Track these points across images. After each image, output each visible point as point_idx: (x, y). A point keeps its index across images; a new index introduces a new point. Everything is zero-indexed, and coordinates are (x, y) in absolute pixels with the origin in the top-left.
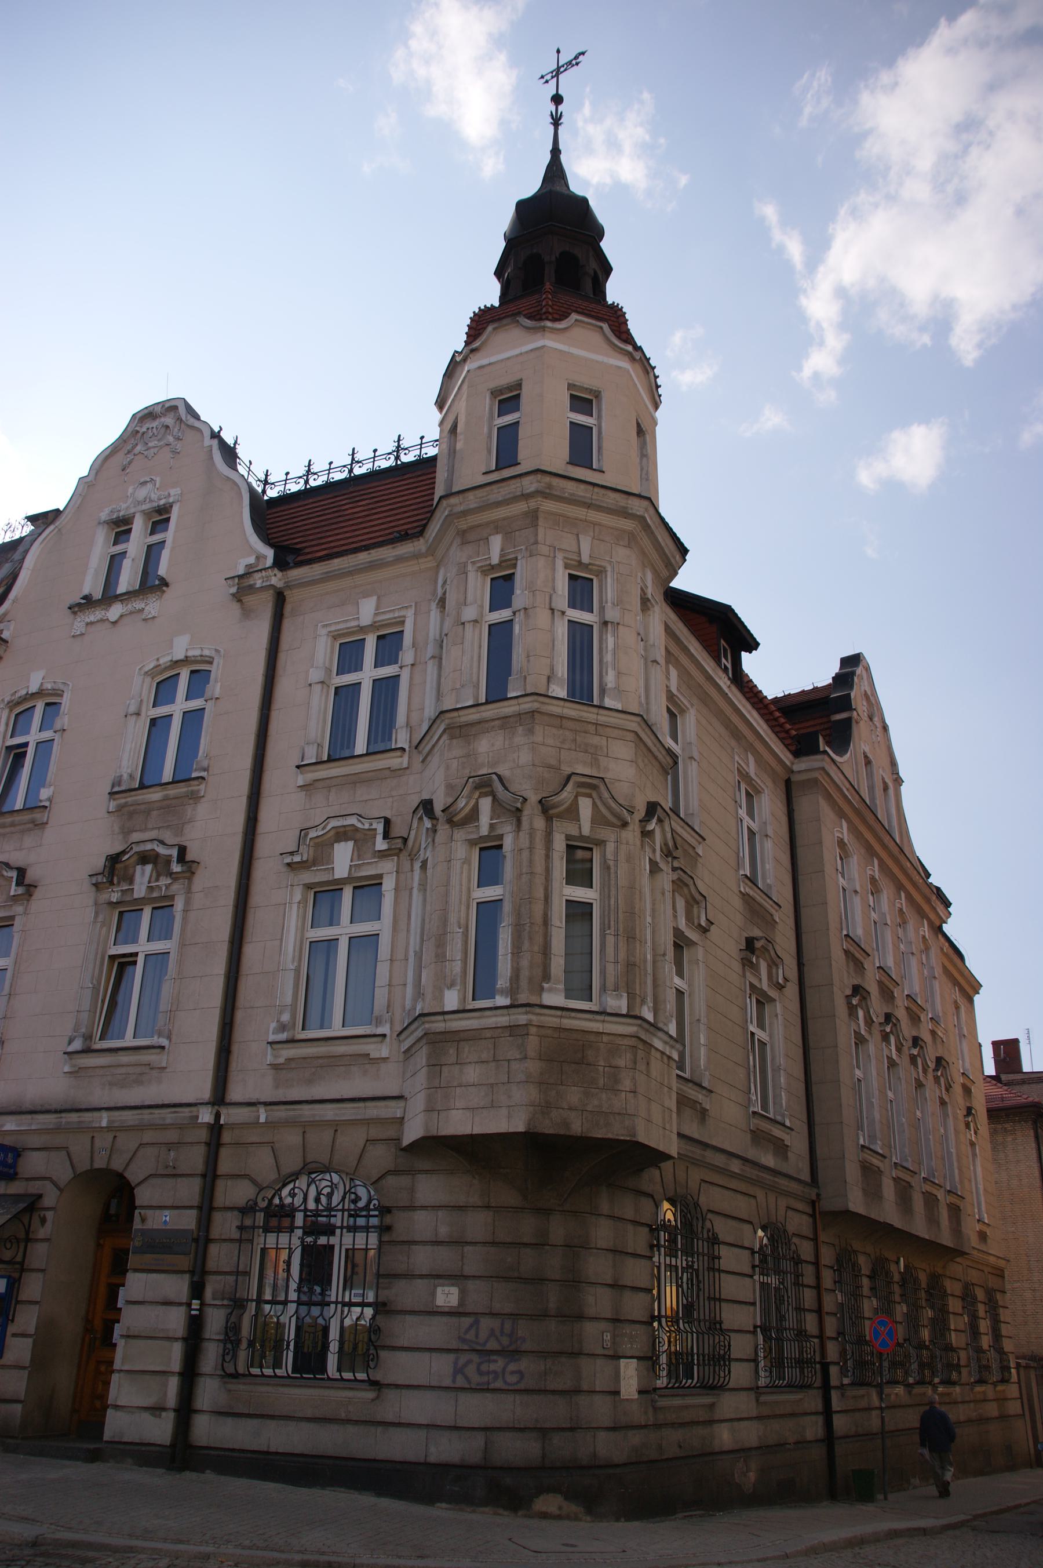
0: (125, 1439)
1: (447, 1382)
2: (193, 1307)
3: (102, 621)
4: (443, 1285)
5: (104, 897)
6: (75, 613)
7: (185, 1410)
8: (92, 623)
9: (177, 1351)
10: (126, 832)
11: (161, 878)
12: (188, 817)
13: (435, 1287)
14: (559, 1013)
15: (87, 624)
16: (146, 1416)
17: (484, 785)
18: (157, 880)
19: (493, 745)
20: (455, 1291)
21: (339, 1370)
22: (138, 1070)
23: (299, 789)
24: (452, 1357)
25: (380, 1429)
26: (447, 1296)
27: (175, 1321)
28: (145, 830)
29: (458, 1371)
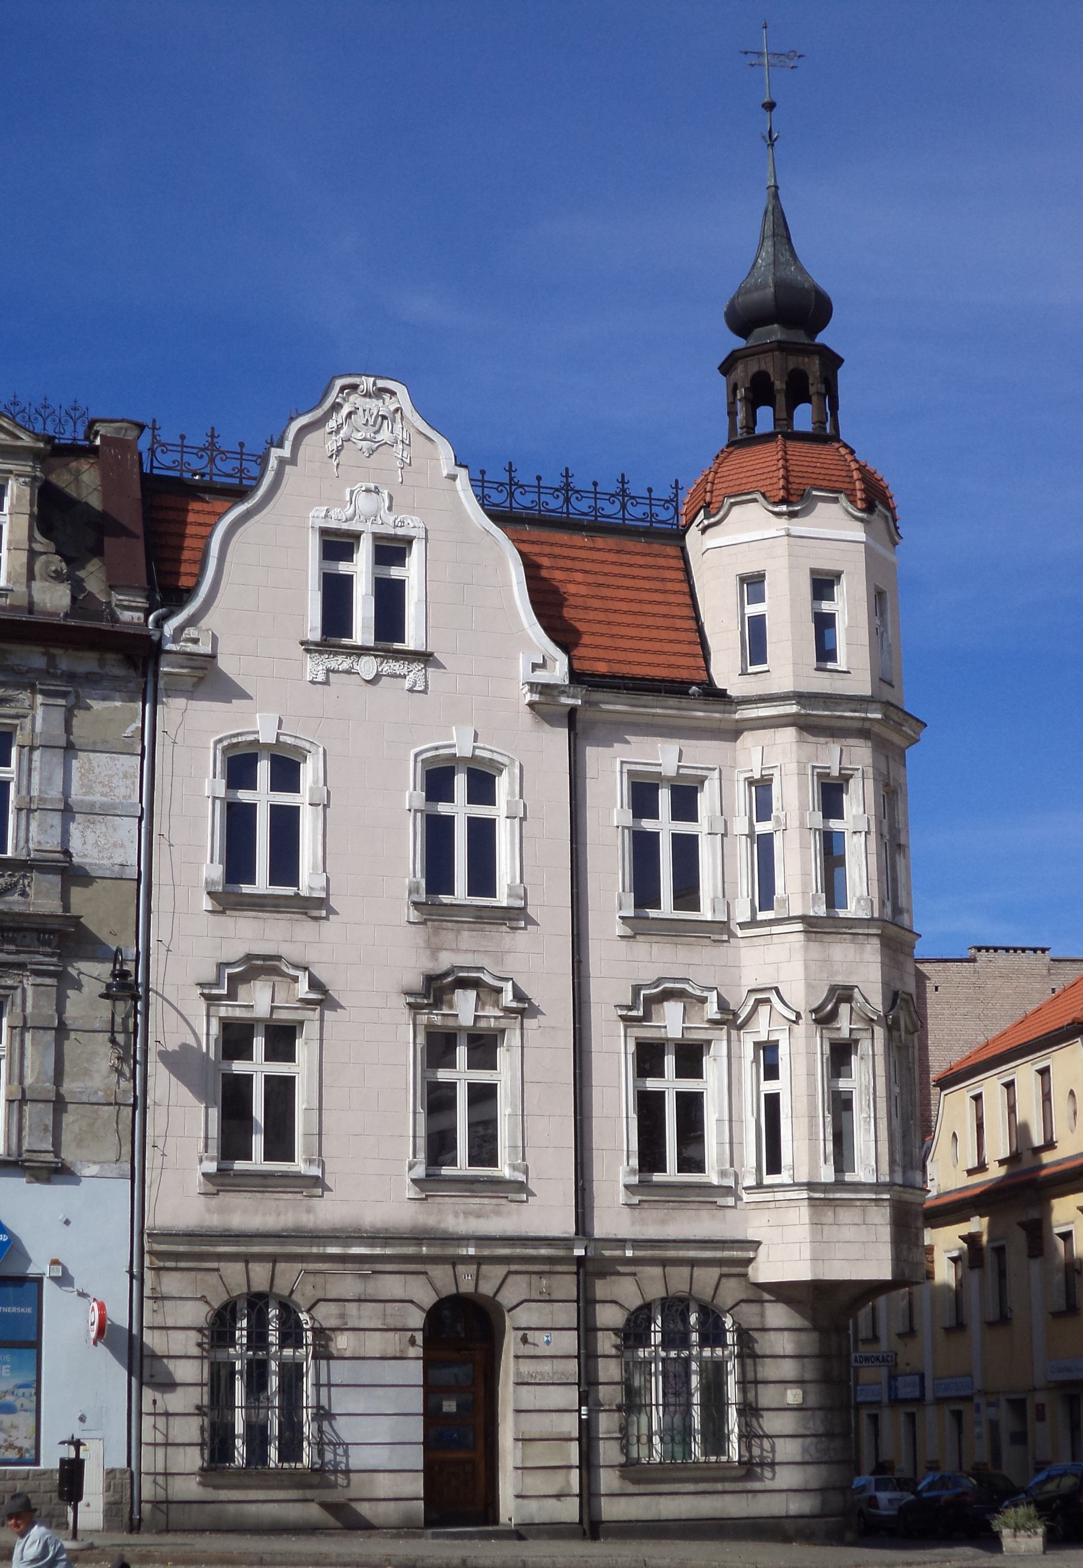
0: (537, 1521)
1: (798, 1459)
2: (583, 1412)
3: (348, 672)
4: (791, 1389)
5: (423, 1019)
7: (588, 1494)
8: (333, 671)
9: (574, 1447)
10: (434, 951)
11: (487, 1008)
12: (507, 947)
13: (786, 1390)
14: (902, 1189)
15: (329, 671)
16: (553, 1501)
17: (842, 994)
18: (483, 1009)
19: (846, 956)
20: (799, 1392)
21: (705, 1453)
22: (494, 1201)
23: (619, 939)
24: (800, 1440)
25: (750, 1495)
26: (793, 1396)
27: (570, 1425)
28: (456, 950)
29: (805, 1450)
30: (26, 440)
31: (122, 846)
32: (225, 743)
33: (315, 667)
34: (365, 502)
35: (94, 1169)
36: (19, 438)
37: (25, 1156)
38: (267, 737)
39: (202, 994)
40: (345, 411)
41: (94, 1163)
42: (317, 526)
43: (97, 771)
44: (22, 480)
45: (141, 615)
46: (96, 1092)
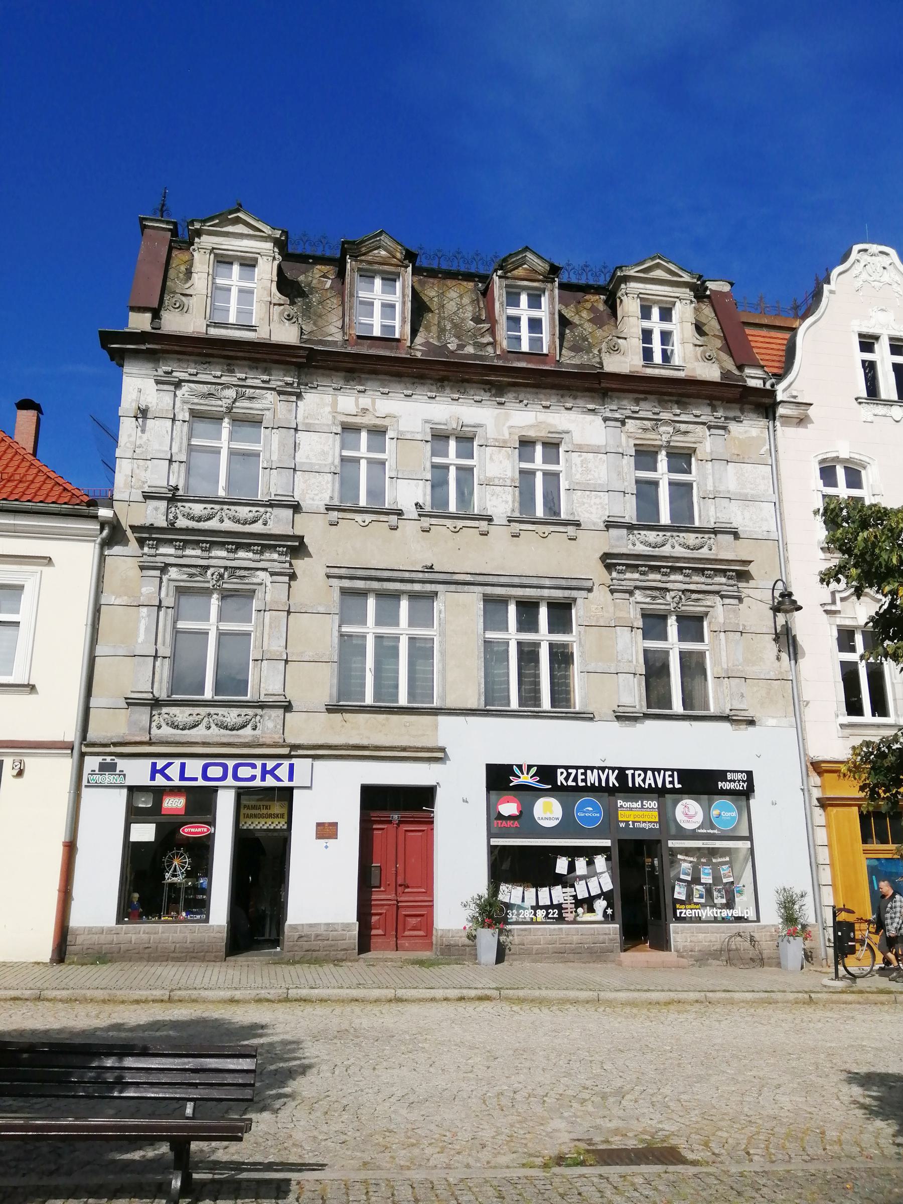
6: (860, 403)
30: (686, 278)
31: (766, 520)
32: (820, 457)
33: (869, 411)
34: (882, 317)
35: (772, 722)
36: (682, 277)
37: (733, 713)
38: (844, 455)
39: (825, 611)
40: (862, 264)
41: (773, 717)
42: (856, 331)
43: (746, 475)
44: (684, 302)
45: (761, 382)
46: (769, 673)
